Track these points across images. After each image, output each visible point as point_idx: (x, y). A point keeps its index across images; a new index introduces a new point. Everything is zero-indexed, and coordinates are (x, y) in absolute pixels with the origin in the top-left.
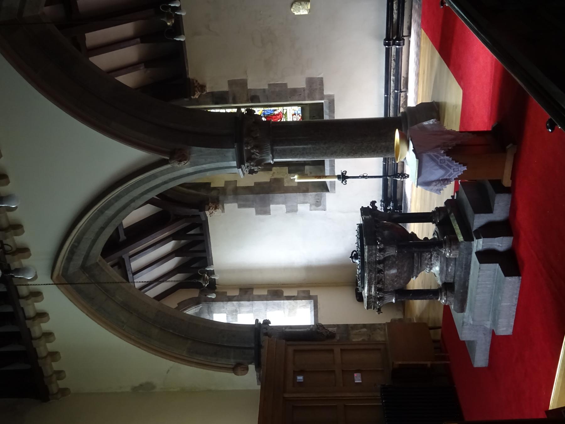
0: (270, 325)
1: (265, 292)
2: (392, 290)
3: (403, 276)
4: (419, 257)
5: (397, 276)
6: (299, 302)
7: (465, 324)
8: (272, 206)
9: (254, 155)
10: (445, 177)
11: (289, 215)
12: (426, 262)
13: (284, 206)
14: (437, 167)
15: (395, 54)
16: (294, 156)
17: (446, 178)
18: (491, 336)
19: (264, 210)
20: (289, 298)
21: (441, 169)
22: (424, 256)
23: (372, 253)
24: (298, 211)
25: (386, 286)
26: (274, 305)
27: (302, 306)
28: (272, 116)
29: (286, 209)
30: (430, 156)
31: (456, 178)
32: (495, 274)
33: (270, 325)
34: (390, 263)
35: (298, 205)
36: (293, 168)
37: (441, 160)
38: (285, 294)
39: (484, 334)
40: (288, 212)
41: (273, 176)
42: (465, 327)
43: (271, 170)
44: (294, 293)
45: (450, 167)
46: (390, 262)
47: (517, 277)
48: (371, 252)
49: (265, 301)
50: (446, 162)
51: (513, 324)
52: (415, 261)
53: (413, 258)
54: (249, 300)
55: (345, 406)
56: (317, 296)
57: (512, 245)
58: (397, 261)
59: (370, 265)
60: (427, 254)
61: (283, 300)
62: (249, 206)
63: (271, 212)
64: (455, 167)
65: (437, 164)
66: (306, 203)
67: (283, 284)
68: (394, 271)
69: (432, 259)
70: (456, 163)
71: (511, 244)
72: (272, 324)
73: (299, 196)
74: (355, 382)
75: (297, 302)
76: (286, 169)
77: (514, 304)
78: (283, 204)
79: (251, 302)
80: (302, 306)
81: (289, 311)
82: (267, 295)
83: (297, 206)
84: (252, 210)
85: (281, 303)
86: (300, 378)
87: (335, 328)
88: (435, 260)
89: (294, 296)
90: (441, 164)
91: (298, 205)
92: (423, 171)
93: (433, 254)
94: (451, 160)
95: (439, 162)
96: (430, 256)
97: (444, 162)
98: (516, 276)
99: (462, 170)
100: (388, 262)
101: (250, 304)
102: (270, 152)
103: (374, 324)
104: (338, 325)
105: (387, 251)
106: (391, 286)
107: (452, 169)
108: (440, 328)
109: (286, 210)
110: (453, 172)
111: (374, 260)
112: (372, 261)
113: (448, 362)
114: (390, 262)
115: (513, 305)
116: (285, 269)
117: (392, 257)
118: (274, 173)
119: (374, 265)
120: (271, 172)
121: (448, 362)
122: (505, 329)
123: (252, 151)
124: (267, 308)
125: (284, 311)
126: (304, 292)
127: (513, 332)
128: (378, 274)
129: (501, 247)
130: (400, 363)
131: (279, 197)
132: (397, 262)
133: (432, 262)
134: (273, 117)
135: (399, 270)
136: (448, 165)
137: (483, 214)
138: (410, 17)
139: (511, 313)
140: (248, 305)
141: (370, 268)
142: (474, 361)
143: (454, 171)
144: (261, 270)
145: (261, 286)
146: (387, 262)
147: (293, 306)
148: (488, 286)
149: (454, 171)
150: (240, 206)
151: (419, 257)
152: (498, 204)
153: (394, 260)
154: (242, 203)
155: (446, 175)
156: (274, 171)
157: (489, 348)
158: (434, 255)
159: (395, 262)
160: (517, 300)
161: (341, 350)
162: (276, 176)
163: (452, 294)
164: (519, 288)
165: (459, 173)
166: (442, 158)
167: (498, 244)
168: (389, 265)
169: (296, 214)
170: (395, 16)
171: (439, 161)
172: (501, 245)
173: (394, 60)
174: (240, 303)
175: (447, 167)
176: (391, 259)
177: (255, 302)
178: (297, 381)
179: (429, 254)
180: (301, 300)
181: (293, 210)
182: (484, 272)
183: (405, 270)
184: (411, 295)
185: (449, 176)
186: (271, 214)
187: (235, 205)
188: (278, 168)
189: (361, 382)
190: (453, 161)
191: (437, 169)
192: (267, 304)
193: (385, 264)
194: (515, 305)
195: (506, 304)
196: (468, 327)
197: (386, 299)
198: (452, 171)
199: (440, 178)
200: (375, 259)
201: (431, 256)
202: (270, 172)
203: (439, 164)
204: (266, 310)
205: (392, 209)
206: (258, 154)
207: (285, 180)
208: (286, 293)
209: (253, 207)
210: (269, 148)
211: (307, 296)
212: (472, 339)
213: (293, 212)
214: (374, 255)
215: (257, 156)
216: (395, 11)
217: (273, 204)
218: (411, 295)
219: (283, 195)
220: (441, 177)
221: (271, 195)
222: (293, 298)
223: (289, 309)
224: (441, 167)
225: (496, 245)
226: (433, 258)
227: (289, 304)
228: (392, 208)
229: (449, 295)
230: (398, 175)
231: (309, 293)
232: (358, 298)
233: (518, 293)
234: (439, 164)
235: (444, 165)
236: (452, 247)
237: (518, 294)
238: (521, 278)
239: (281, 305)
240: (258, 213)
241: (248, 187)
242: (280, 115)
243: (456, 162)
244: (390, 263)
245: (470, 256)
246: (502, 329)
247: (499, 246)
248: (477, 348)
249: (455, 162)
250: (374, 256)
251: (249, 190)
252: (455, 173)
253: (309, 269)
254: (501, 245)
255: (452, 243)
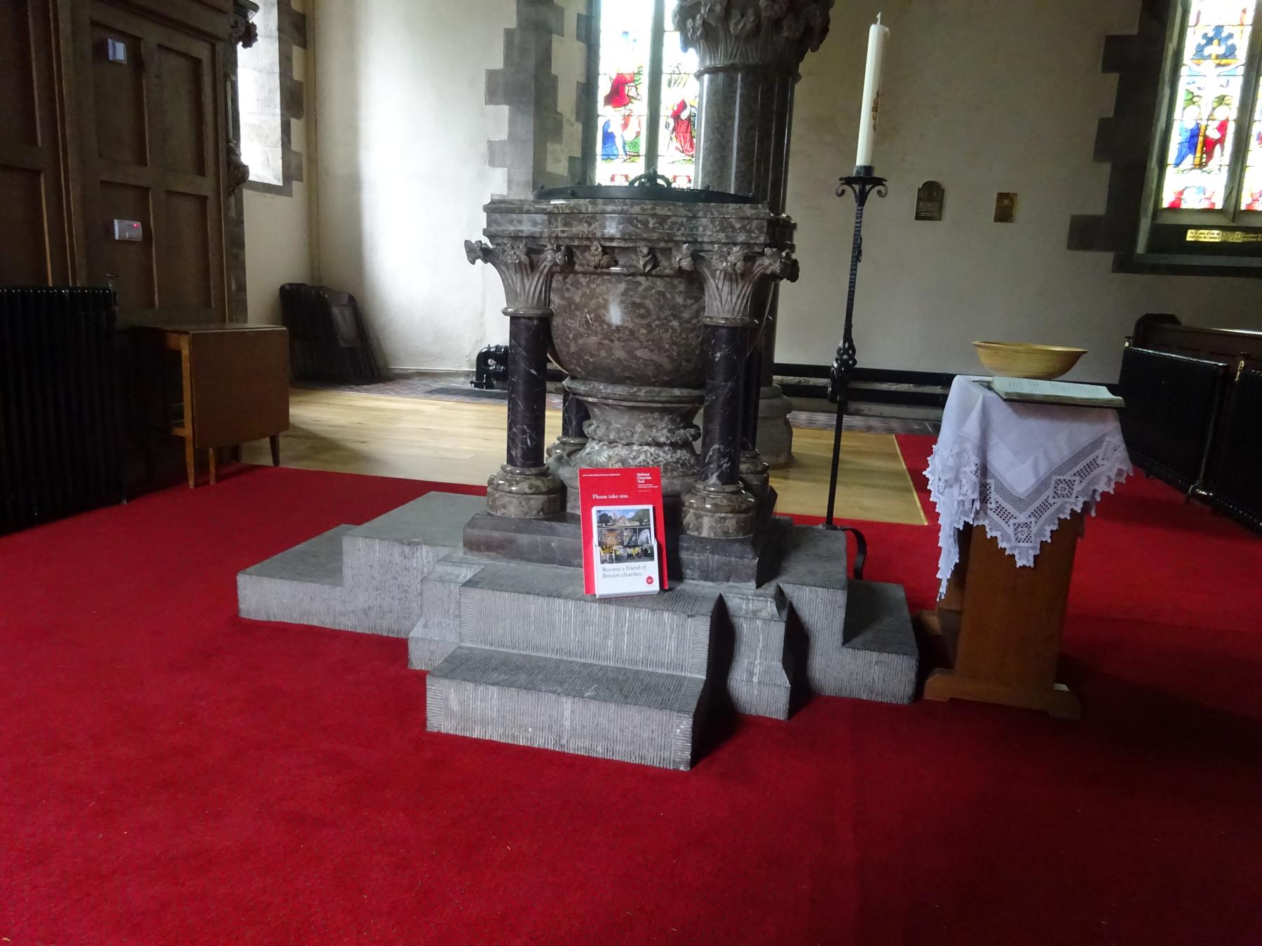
0: (241, 43)
1: (297, 75)
2: (552, 307)
3: (617, 343)
4: (667, 405)
5: (600, 319)
6: (278, 152)
7: (407, 549)
8: (505, 110)
9: (739, 17)
10: (994, 495)
11: (483, 147)
12: (639, 428)
13: (504, 136)
14: (1043, 470)
15: (811, 384)
16: (717, 125)
17: (992, 500)
18: (359, 630)
19: (498, 88)
20: (286, 128)
21: (1037, 482)
22: (662, 419)
23: (733, 227)
24: (491, 168)
25: (583, 280)
26: (270, 91)
27: (267, 158)
28: (691, 133)
29: (497, 140)
30: (1096, 444)
31: (986, 533)
32: (662, 665)
33: (241, 43)
34: (676, 296)
35: (506, 169)
36: (578, 166)
37: (1070, 484)
38: (294, 121)
39: (366, 612)
40: (491, 144)
41: (567, 120)
42: (397, 549)
43: (577, 119)
44: (297, 144)
45: (1037, 514)
46: (680, 300)
47: (687, 755)
48: (738, 226)
49: (278, 71)
50: (1059, 501)
51: (475, 736)
52: (657, 389)
53: (670, 384)
54: (280, 29)
55: (38, 173)
56: (290, 195)
57: (750, 716)
58: (681, 325)
59: (685, 219)
60: (665, 431)
61: (282, 115)
62: (508, 57)
63: (490, 107)
64: (1034, 529)
65: (1060, 470)
66: (509, 188)
67: (316, 120)
68: (615, 315)
69: (646, 448)
70: (1048, 534)
71: (753, 712)
72: (242, 52)
73: (525, 173)
74: (116, 221)
75: (277, 147)
76: (578, 154)
77: (564, 742)
78: (510, 135)
79: (276, 33)
80: (267, 158)
81: (254, 126)
82: (291, 78)
83: (503, 167)
84: (498, 63)
85: (275, 107)
86: (119, 51)
87: (234, 212)
88: (646, 457)
89: (289, 141)
90: (1053, 483)
91: (506, 169)
92: (1036, 425)
93: (664, 452)
94: (1062, 517)
95: (1061, 478)
96: (662, 439)
97: (1059, 492)
98: (692, 754)
99: (1016, 553)
100: (681, 292)
101: (271, 30)
102: (737, 61)
103: (246, 308)
104: (242, 222)
105: (735, 285)
106: (577, 299)
107: (1028, 521)
108: (276, 460)
109: (496, 141)
110: (1016, 521)
111: (702, 236)
112: (697, 228)
113: (191, 483)
114: (680, 300)
115: (560, 738)
116: (353, 129)
117: (695, 307)
118: (572, 125)
119: (683, 235)
120: (573, 119)
121: (191, 483)
122: (455, 706)
123: (750, 12)
124: (260, 71)
125: (254, 113)
126: (300, 168)
127: (439, 734)
128: (645, 251)
129: (750, 681)
130: (186, 352)
131: (527, 126)
132: (675, 323)
133: (635, 447)
134: (688, 135)
135: (644, 331)
136: (1045, 506)
137: (843, 616)
138: (879, 414)
139: (526, 730)
140: (268, 25)
141: (674, 219)
142: (260, 574)
143: (1017, 526)
144: (352, 70)
145: (311, 65)
146: (682, 288)
147: (267, 137)
148: (610, 643)
149: (1017, 526)
150: (509, 34)
151: (667, 405)
152: (876, 663)
153: (686, 315)
154: (517, 40)
155: (1005, 499)
156: (575, 126)
157: (315, 623)
158: (661, 453)
159: (675, 317)
160: (583, 753)
161: (205, 198)
162: (566, 128)
163: (535, 512)
164: (638, 761)
165: (1009, 540)
166: (1077, 488)
167: (756, 670)
168: (668, 296)
169: (485, 164)
170: (885, 386)
171: (1067, 477)
172: (755, 679)
173: (800, 381)
174: (273, 5)
175: (1037, 504)
176: (689, 302)
177: (277, 45)
178: (110, 41)
179: (667, 438)
180: (283, 158)
181: (494, 155)
182: (672, 631)
183: (639, 353)
184: (533, 372)
185: (1000, 510)
186: (488, 106)
187: (512, 23)
188: (581, 136)
189: (117, 238)
190: (1057, 522)
191: (1035, 468)
192: (271, 73)
193: (676, 282)
194: (561, 746)
195: (567, 713)
196: (397, 558)
197: (526, 281)
198: (1022, 518)
199: (993, 477)
200: (706, 239)
201: (659, 445)
202: (574, 117)
203: (1055, 478)
204: (255, 69)
205: (489, 369)
206: (740, 26)
207: (557, 146)
208: (295, 124)
209: (505, 64)
210: (749, 60)
211: (289, 174)
212: (347, 572)
213: (491, 155)
214: (727, 237)
215: (737, 24)
216: (893, 387)
217: (510, 110)
218: (533, 372)
219: (531, 136)
220: (998, 482)
221: (532, 108)
222: (286, 140)
223: (259, 126)
224: (1042, 485)
225: (752, 664)
226: (652, 450)
227: (272, 126)
228: (491, 368)
229: (532, 502)
230: (850, 352)
231: (297, 180)
232: (288, 288)
233: (617, 758)
234: (1055, 478)
235: (1050, 492)
236: (730, 515)
237: (609, 756)
238: (682, 768)
239: (269, 106)
240: (491, 75)
241: (550, 59)
242: (690, 149)
243: (1052, 531)
244: (676, 296)
245: (696, 575)
246: (452, 695)
247: (751, 674)
248: (314, 588)
249: (1055, 529)
250: (722, 236)
251: (545, 59)
252: (1010, 531)
253: (354, 183)
254: (755, 679)
255: (743, 516)
